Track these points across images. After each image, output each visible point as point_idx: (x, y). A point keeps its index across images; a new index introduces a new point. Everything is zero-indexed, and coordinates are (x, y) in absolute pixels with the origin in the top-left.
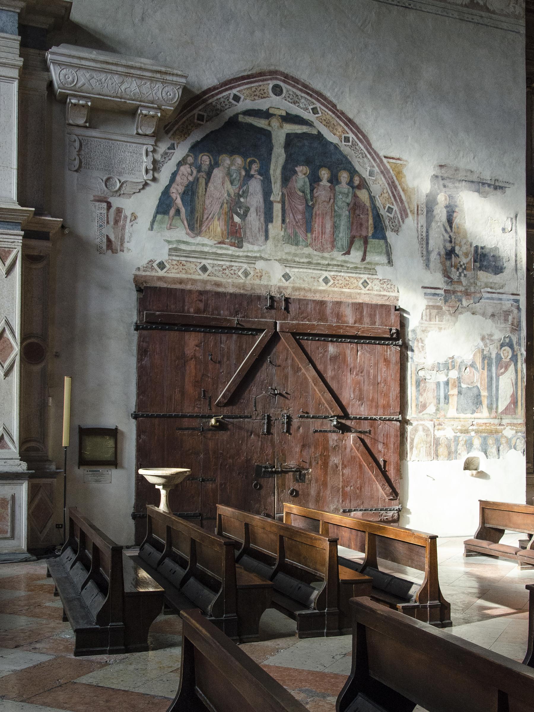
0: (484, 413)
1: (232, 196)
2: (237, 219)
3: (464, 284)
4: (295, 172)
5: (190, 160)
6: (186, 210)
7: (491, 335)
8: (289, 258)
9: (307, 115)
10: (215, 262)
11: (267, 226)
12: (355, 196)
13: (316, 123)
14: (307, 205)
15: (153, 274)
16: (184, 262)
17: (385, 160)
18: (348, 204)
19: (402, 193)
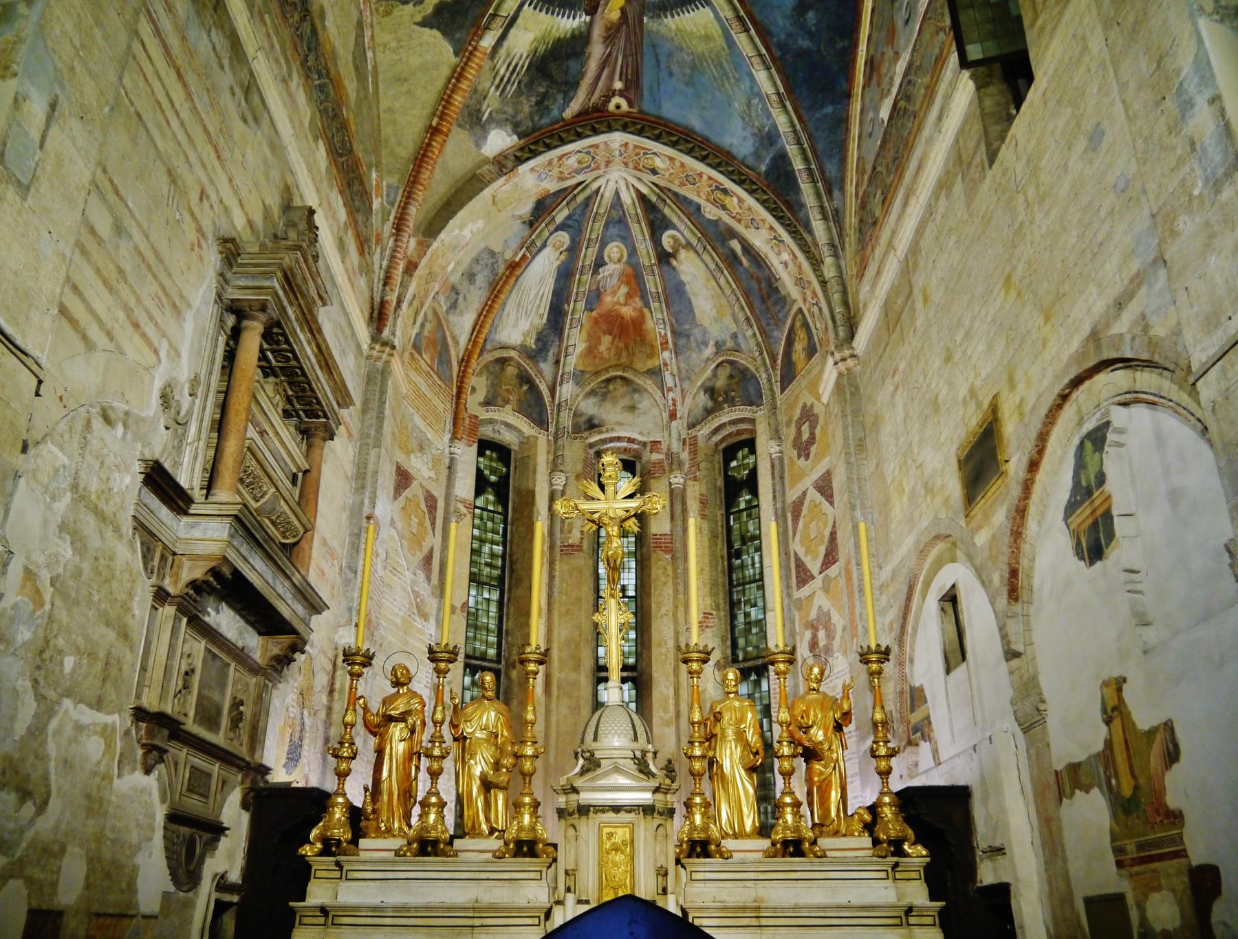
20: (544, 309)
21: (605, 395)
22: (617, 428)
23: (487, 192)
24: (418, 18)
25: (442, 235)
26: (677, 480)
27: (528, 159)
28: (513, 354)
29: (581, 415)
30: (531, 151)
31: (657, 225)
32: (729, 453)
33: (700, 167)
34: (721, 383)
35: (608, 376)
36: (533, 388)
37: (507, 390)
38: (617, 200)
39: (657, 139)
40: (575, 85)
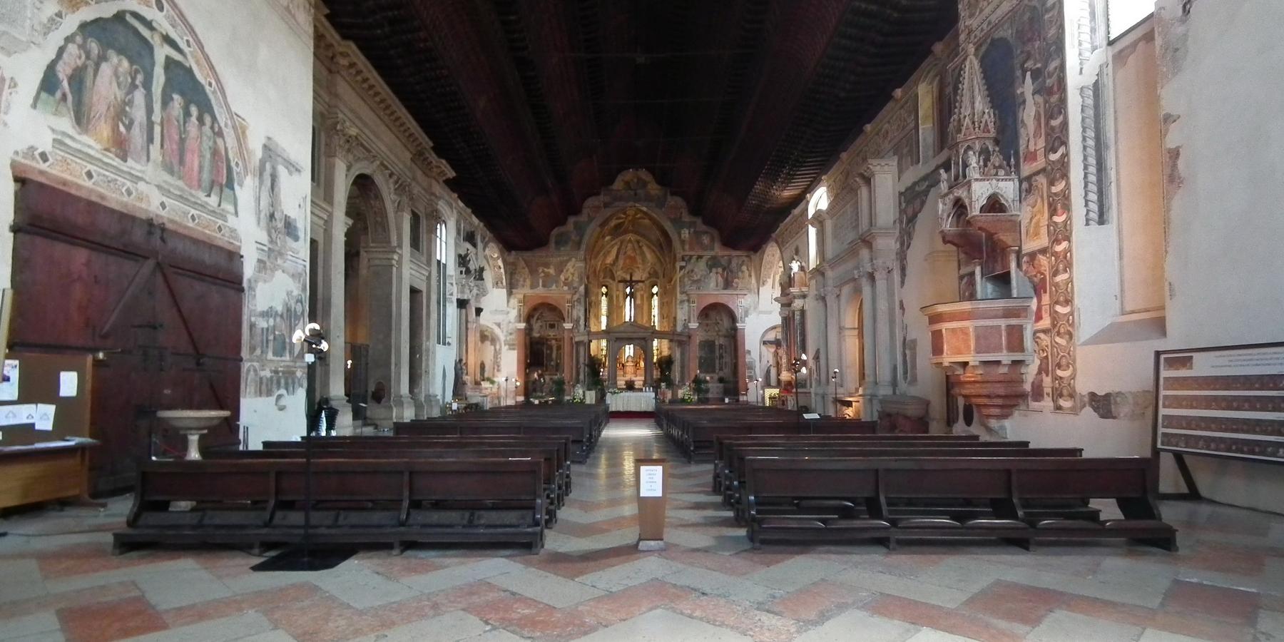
0: (287, 357)
1: (119, 99)
2: (122, 129)
3: (279, 245)
4: (172, 99)
5: (79, 39)
6: (73, 97)
7: (292, 292)
8: (166, 187)
9: (183, 45)
10: (101, 171)
11: (148, 146)
12: (215, 142)
13: (189, 57)
14: (181, 137)
15: (34, 164)
16: (69, 161)
17: (235, 117)
18: (210, 148)
19: (245, 152)
20: (615, 255)
26: (642, 292)
31: (638, 242)
32: (653, 287)
34: (651, 272)
36: (613, 274)
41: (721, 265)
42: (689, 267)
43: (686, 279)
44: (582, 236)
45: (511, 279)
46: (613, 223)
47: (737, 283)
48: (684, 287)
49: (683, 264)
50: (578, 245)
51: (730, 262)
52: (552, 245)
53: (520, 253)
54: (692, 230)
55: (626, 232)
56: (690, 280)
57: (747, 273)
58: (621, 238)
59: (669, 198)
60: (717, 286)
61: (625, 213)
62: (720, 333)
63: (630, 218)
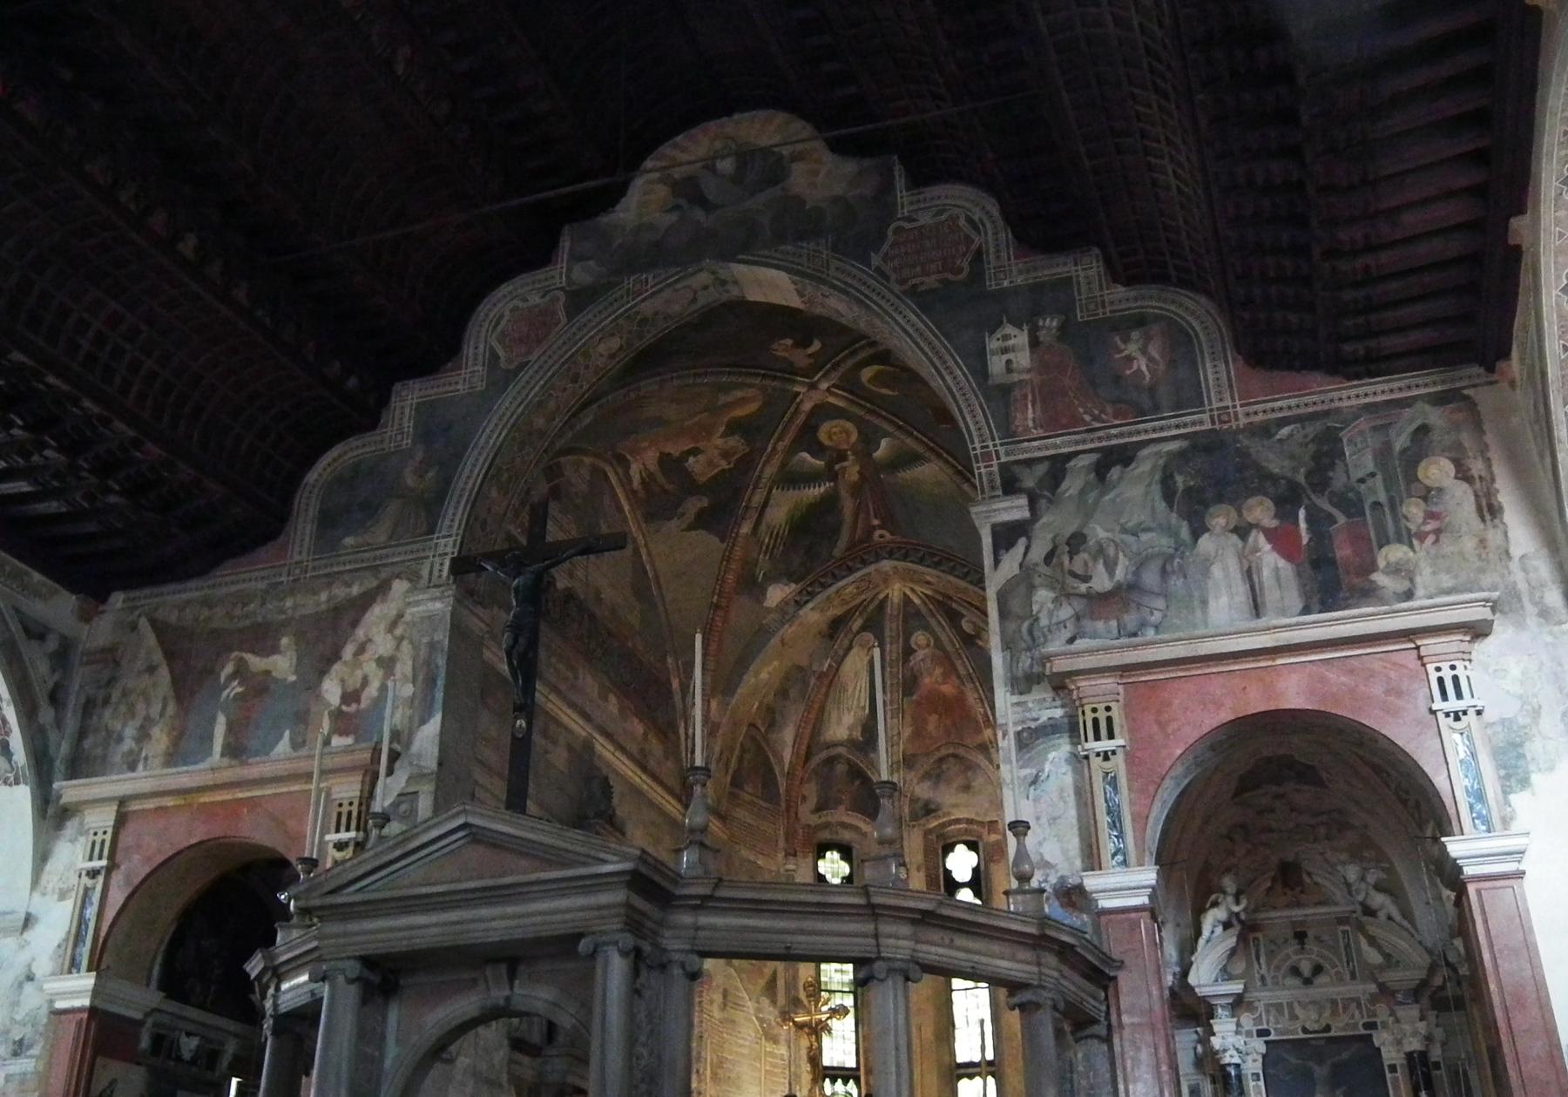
21: (938, 776)
22: (954, 811)
23: (775, 641)
24: (684, 526)
25: (739, 691)
27: (807, 602)
28: (841, 750)
29: (919, 799)
30: (809, 593)
31: (954, 617)
33: (963, 584)
35: (938, 755)
37: (839, 791)
38: (907, 601)
39: (921, 561)
40: (836, 530)
41: (1262, 481)
42: (1054, 524)
43: (1043, 596)
44: (448, 469)
45: (82, 734)
46: (782, 509)
47: (1397, 570)
48: (1034, 643)
49: (1014, 509)
50: (430, 507)
51: (1327, 452)
52: (303, 527)
53: (147, 597)
54: (1050, 323)
55: (863, 552)
56: (1065, 595)
57: (1460, 501)
58: (847, 586)
59: (903, 196)
60: (1257, 609)
61: (818, 449)
62: (1392, 977)
63: (852, 470)
